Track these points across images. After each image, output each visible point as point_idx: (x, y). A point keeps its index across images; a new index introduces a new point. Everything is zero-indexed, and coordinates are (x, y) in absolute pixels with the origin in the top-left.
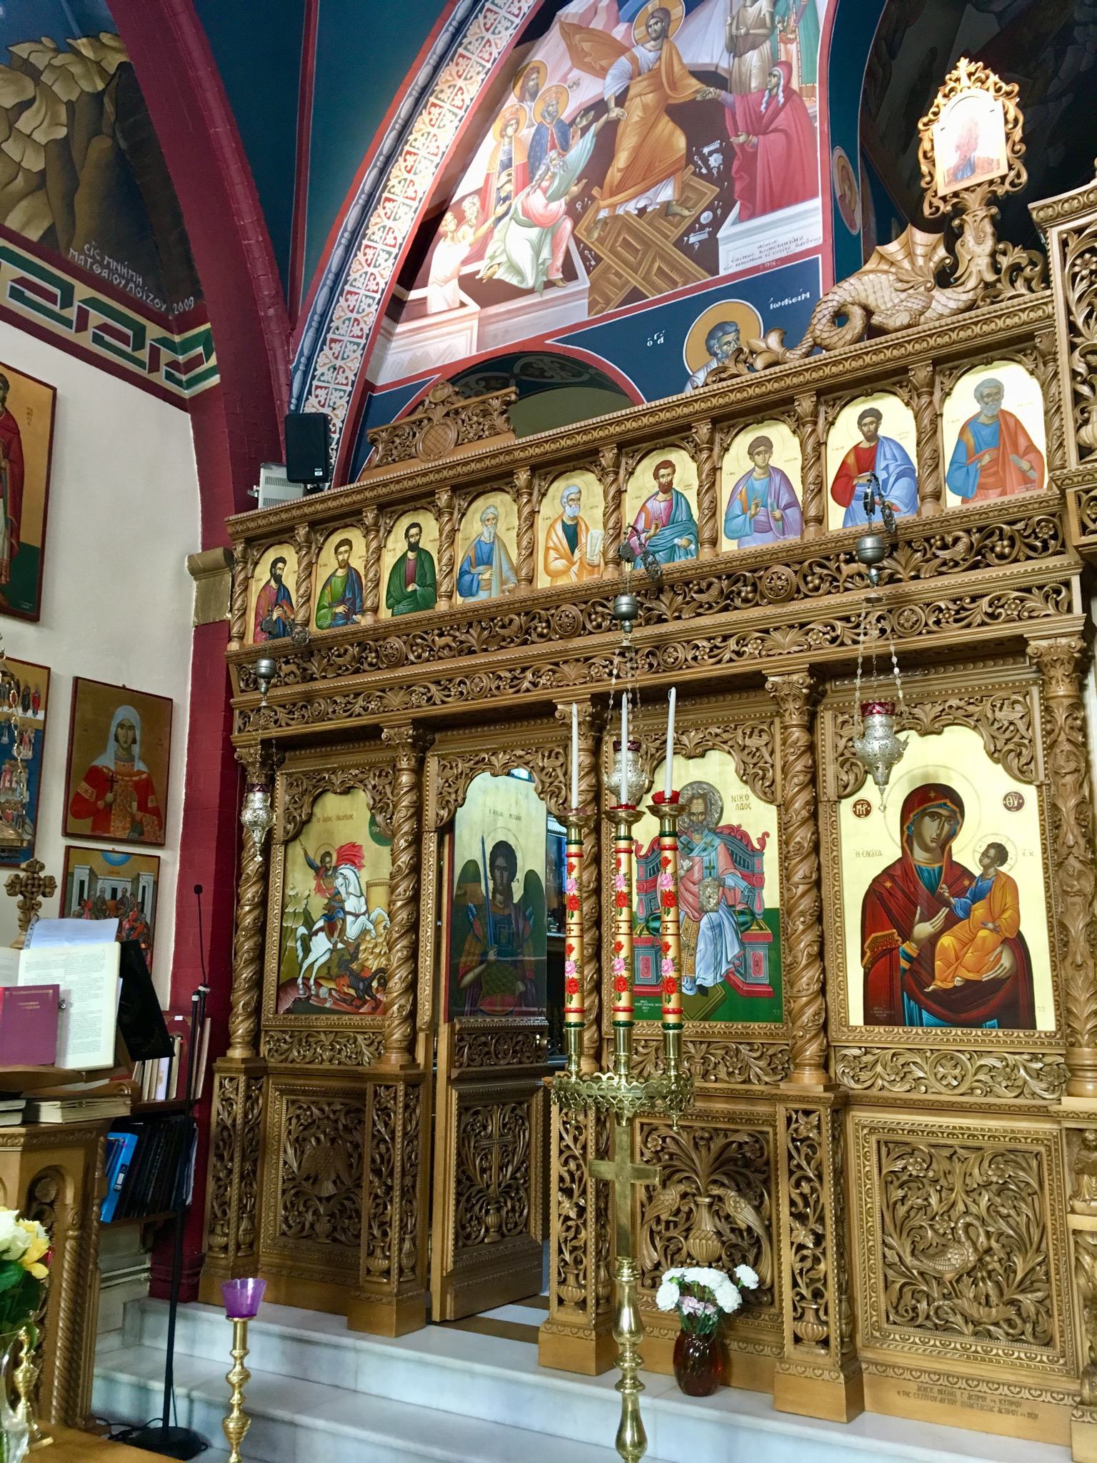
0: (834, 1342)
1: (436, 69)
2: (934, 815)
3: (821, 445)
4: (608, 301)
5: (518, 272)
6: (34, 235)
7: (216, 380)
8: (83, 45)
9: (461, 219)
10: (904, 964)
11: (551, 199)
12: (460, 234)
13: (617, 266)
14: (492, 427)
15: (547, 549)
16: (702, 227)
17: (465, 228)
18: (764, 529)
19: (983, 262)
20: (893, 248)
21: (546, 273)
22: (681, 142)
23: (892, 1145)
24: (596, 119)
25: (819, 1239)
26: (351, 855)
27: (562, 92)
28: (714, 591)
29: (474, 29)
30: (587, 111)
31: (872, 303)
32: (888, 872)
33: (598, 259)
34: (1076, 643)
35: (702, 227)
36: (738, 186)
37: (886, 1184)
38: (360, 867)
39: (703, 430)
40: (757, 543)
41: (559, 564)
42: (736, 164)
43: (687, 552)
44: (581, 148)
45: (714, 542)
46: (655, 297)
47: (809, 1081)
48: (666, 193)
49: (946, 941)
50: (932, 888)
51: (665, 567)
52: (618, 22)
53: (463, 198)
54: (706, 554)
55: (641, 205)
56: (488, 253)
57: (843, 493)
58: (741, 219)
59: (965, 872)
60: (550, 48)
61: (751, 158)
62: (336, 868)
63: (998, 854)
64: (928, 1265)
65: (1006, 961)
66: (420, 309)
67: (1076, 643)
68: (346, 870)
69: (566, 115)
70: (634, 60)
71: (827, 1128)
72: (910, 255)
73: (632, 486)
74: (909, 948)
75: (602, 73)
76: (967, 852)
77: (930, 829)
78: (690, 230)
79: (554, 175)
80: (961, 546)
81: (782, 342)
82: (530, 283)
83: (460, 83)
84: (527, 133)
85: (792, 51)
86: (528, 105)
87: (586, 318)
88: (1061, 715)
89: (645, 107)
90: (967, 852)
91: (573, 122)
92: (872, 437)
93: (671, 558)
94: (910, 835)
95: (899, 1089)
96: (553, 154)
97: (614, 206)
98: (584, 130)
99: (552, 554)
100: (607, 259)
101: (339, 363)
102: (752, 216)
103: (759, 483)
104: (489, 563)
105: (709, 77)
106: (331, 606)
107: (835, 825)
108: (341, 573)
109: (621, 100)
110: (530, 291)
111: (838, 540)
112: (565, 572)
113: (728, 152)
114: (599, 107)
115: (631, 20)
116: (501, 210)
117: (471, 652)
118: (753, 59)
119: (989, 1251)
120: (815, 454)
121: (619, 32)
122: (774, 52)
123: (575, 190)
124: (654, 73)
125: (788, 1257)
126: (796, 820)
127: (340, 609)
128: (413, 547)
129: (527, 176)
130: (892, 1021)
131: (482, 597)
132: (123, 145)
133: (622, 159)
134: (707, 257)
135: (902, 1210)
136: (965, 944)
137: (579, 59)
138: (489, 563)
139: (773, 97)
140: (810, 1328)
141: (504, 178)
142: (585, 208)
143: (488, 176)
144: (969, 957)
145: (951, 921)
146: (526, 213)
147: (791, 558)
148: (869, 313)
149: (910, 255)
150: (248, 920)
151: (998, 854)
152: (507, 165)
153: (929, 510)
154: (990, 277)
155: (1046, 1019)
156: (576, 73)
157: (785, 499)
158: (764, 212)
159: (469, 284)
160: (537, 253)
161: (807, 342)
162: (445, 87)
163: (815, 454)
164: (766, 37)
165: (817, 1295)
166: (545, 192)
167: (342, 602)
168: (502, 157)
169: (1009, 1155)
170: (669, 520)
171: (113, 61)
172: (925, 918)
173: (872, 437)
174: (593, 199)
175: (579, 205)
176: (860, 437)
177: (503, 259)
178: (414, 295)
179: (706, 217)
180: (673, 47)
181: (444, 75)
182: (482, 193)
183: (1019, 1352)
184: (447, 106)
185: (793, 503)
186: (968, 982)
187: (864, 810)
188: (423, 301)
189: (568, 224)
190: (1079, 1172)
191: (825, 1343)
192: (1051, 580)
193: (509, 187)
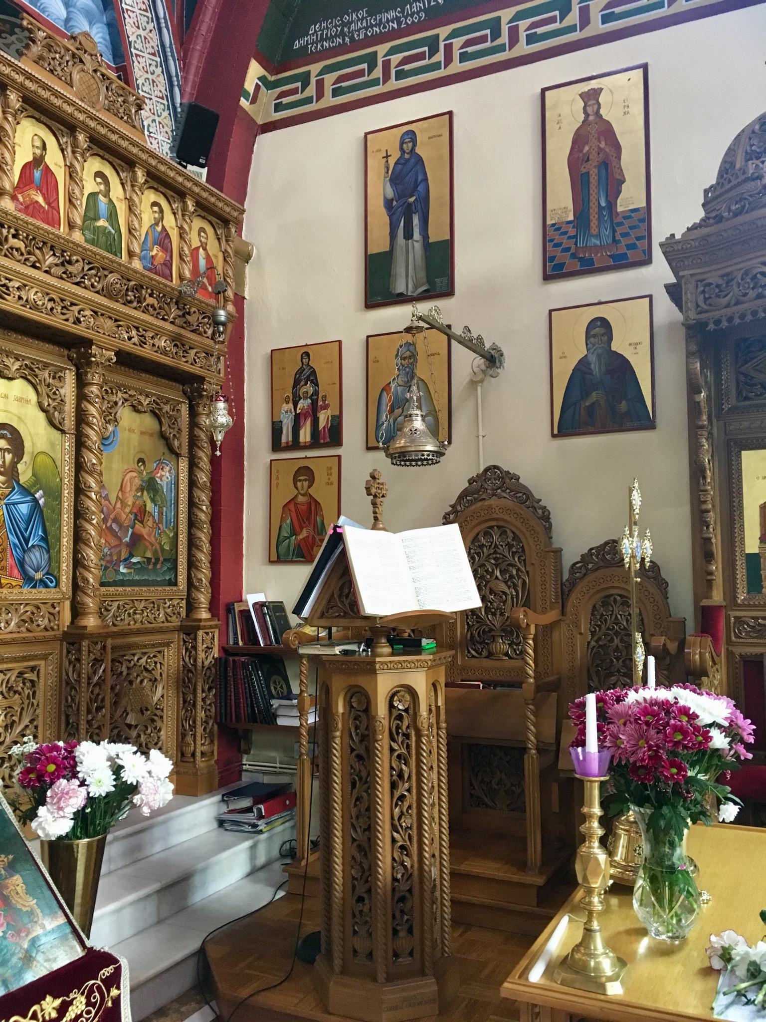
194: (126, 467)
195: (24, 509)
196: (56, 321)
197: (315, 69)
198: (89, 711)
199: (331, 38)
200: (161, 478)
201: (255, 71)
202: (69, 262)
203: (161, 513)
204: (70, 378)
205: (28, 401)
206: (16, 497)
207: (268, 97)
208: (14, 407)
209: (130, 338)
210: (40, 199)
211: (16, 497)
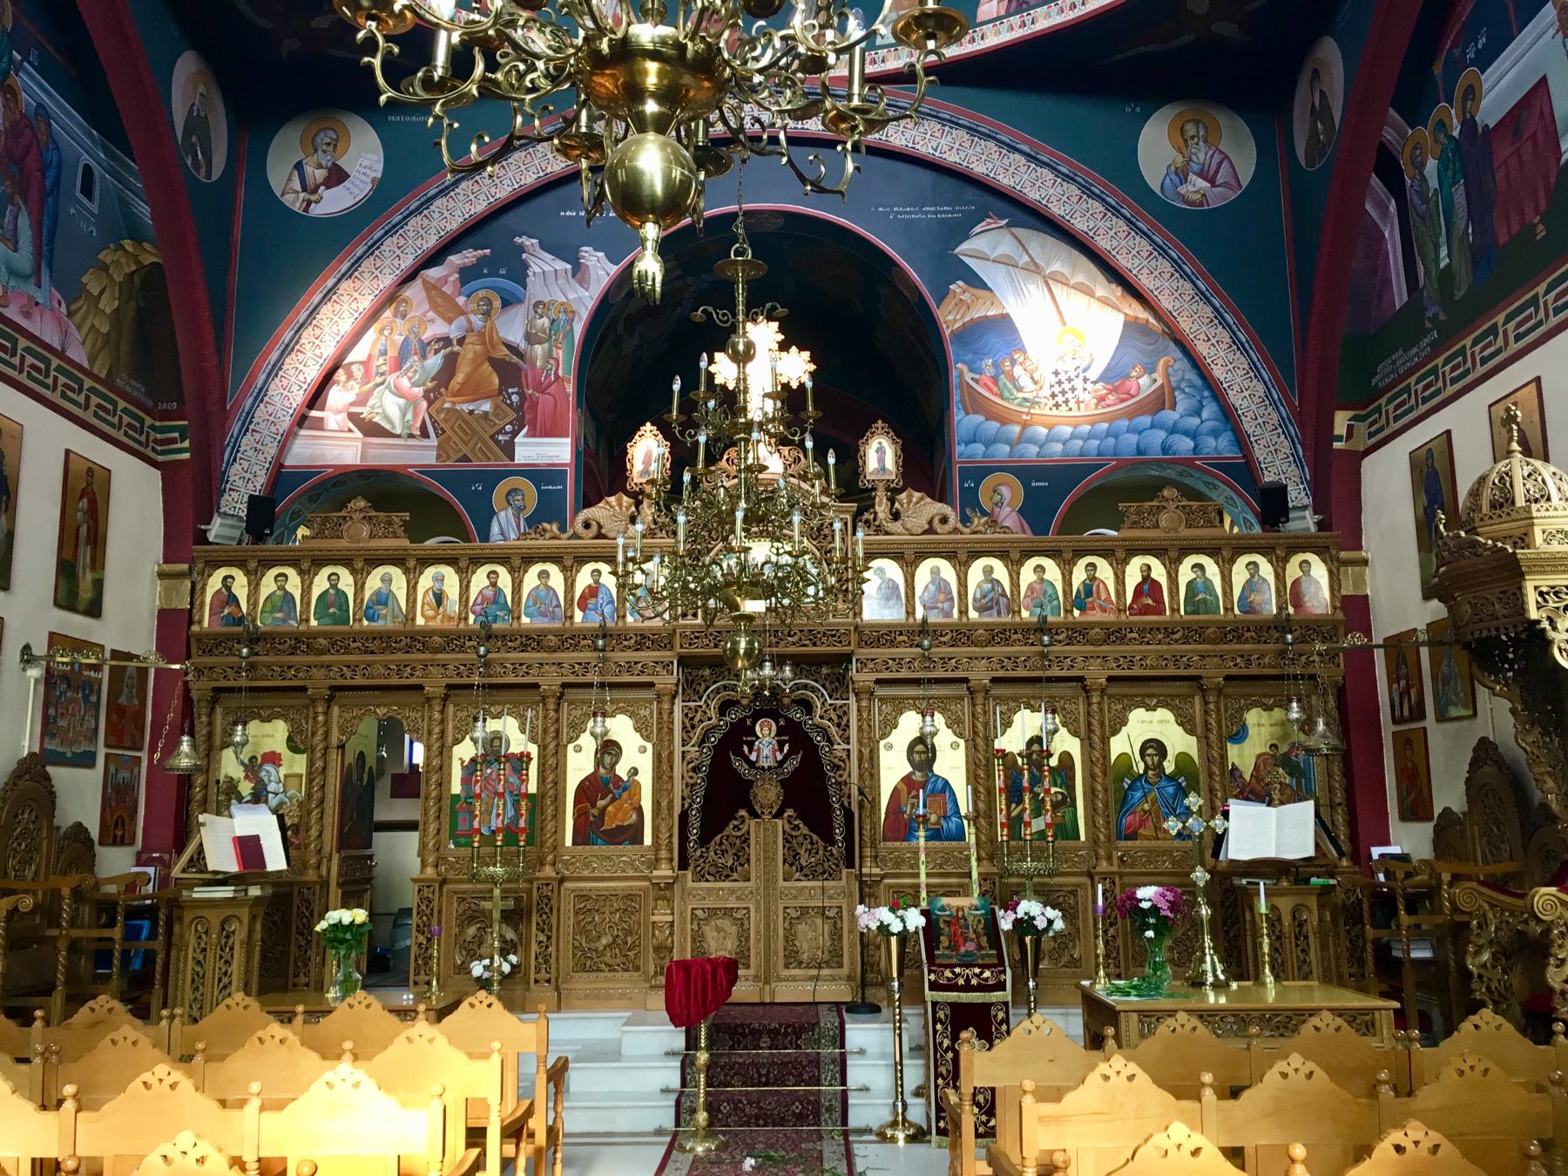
0: (553, 980)
1: (339, 280)
2: (610, 754)
3: (573, 582)
4: (449, 458)
5: (390, 421)
6: (103, 375)
7: (187, 456)
8: (128, 244)
9: (350, 376)
10: (592, 819)
11: (415, 385)
12: (349, 385)
13: (455, 438)
14: (394, 532)
15: (423, 604)
16: (506, 433)
17: (352, 383)
18: (543, 615)
19: (650, 518)
20: (612, 499)
21: (409, 428)
22: (496, 381)
23: (582, 897)
24: (444, 347)
25: (549, 938)
26: (273, 758)
27: (423, 322)
28: (518, 642)
29: (367, 264)
30: (439, 340)
31: (602, 522)
32: (587, 778)
33: (444, 431)
34: (674, 688)
35: (506, 433)
36: (527, 417)
37: (576, 913)
38: (280, 765)
39: (517, 562)
40: (543, 623)
41: (431, 613)
42: (526, 405)
43: (504, 620)
44: (435, 362)
45: (519, 618)
46: (478, 463)
47: (548, 871)
48: (486, 406)
49: (610, 808)
50: (607, 785)
51: (494, 626)
52: (460, 294)
53: (352, 363)
54: (515, 625)
55: (471, 408)
56: (371, 402)
57: (583, 605)
58: (527, 435)
59: (620, 779)
60: (414, 291)
61: (535, 405)
62: (261, 765)
63: (634, 771)
64: (592, 946)
65: (634, 817)
66: (319, 424)
67: (674, 688)
68: (269, 767)
69: (426, 337)
70: (469, 321)
71: (556, 890)
72: (620, 505)
73: (474, 579)
74: (595, 812)
75: (450, 321)
76: (622, 770)
77: (608, 759)
78: (499, 432)
79: (415, 371)
80: (633, 641)
81: (559, 529)
82: (398, 431)
83: (356, 295)
84: (399, 339)
85: (560, 354)
86: (399, 321)
87: (433, 462)
88: (665, 717)
89: (475, 352)
90: (622, 770)
91: (429, 344)
92: (597, 582)
93: (495, 622)
94: (598, 763)
95: (586, 873)
96: (416, 358)
97: (454, 403)
98: (437, 352)
99: (426, 607)
100: (449, 432)
101: (259, 447)
102: (534, 436)
103: (543, 593)
104: (385, 604)
105: (513, 349)
106: (271, 612)
107: (565, 756)
108: (280, 593)
109: (461, 341)
110: (399, 436)
111: (580, 629)
112: (434, 618)
113: (521, 394)
114: (446, 341)
115: (468, 296)
116: (379, 380)
117: (372, 652)
118: (539, 349)
119: (618, 936)
120: (570, 585)
121: (461, 300)
122: (550, 352)
123: (430, 385)
124: (481, 335)
125: (534, 947)
126: (550, 753)
127: (279, 615)
128: (334, 586)
129: (398, 364)
130: (587, 844)
131: (379, 624)
132: (142, 304)
133: (459, 378)
134: (509, 450)
135: (583, 924)
136: (618, 810)
137: (434, 306)
138: (385, 604)
139: (548, 376)
140: (543, 975)
141: (381, 361)
142: (436, 398)
143: (370, 356)
144: (620, 815)
145: (613, 800)
146: (396, 387)
147: (556, 633)
148: (600, 527)
149: (620, 505)
150: (198, 797)
151: (634, 771)
152: (384, 353)
153: (620, 623)
154: (653, 527)
155: (648, 840)
156: (431, 314)
157: (554, 603)
158: (541, 436)
159: (353, 417)
160: (404, 415)
161: (570, 532)
162: (345, 293)
163: (570, 585)
164: (547, 341)
165: (546, 962)
166: (410, 379)
167: (280, 611)
168: (379, 347)
169: (630, 897)
170: (495, 601)
171: (148, 259)
172: (602, 799)
173: (597, 582)
174: (441, 394)
175: (432, 395)
176: (591, 581)
177: (380, 410)
178: (314, 413)
179: (509, 428)
180: (493, 326)
181: (344, 285)
182: (366, 364)
183: (626, 974)
184: (346, 306)
185: (558, 606)
186: (618, 826)
187: (578, 749)
188: (322, 419)
189: (425, 404)
190: (656, 900)
191: (549, 981)
192: (667, 660)
193: (384, 368)
194: (1259, 751)
195: (1171, 790)
196: (1171, 671)
197: (1383, 401)
198: (1224, 924)
199: (1387, 376)
200: (1296, 756)
201: (1341, 421)
202: (1173, 633)
203: (1299, 784)
204: (1197, 700)
205: (1167, 722)
206: (1163, 783)
207: (1361, 428)
208: (1156, 726)
209: (1236, 665)
210: (1150, 602)
211: (1163, 783)
